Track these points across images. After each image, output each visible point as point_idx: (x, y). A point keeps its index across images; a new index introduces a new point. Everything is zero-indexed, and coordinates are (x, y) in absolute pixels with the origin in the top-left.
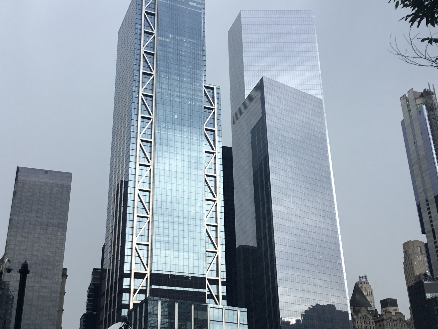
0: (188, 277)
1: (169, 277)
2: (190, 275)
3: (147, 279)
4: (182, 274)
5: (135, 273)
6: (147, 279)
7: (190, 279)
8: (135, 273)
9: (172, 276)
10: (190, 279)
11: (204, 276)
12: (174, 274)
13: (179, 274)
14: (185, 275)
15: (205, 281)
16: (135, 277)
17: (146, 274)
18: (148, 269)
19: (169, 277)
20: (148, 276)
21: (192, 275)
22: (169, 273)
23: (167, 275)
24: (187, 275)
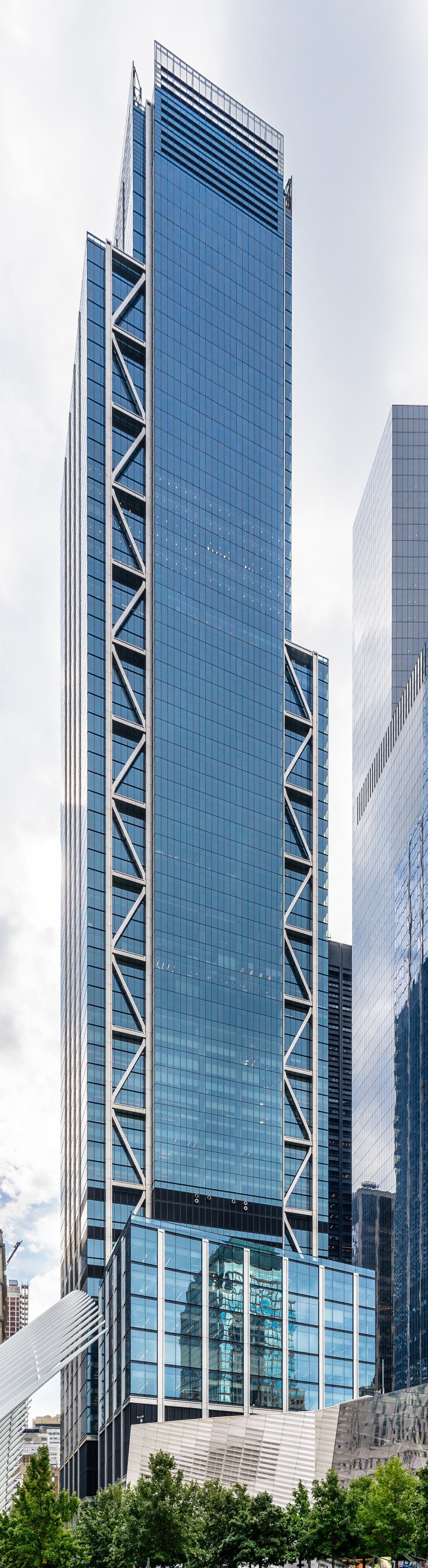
0: (240, 1204)
1: (197, 1201)
2: (246, 1200)
3: (144, 1205)
4: (227, 1196)
5: (116, 1189)
6: (144, 1205)
7: (246, 1208)
8: (116, 1189)
9: (202, 1197)
10: (246, 1208)
11: (278, 1204)
12: (209, 1194)
13: (221, 1195)
14: (234, 1198)
15: (281, 1216)
16: (115, 1200)
17: (141, 1192)
18: (147, 1180)
19: (197, 1201)
20: (147, 1196)
21: (251, 1200)
22: (196, 1192)
23: (191, 1196)
24: (239, 1198)
